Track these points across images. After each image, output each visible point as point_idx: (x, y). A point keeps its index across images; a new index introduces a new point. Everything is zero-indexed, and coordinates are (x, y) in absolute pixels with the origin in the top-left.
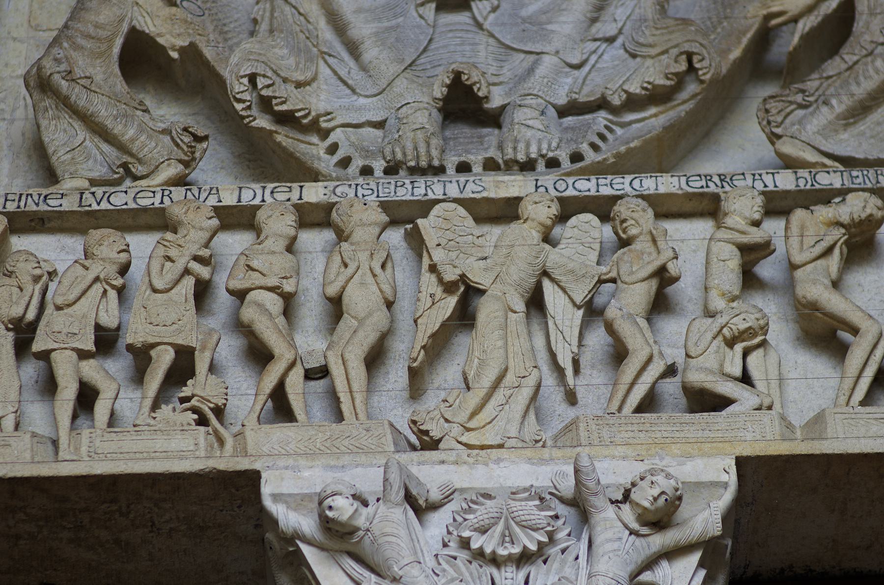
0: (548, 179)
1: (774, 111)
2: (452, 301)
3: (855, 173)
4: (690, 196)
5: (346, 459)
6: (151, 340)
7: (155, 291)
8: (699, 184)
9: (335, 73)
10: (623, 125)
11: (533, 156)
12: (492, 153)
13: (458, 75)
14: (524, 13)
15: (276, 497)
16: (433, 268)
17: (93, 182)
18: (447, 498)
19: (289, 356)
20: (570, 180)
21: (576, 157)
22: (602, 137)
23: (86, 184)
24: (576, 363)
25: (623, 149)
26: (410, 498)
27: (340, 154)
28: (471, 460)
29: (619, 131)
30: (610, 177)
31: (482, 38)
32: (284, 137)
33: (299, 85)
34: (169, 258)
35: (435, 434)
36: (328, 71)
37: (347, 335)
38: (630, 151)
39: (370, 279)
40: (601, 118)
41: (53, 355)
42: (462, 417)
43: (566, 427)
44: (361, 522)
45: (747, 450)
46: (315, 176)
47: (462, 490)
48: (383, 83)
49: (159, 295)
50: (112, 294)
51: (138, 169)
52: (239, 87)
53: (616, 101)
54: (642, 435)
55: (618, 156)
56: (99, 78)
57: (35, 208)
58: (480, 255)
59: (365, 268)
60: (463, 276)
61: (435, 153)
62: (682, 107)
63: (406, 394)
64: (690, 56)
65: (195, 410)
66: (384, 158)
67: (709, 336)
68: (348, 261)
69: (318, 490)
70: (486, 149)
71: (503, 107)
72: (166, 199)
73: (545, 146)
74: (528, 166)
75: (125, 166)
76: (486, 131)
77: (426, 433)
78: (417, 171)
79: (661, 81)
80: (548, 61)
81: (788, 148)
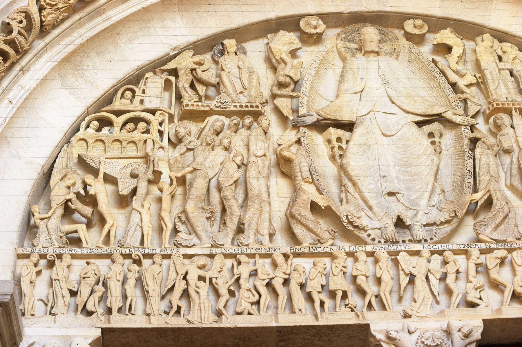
0: (426, 245)
1: (477, 227)
2: (408, 278)
3: (499, 244)
4: (460, 250)
5: (390, 321)
6: (336, 289)
7: (334, 275)
8: (463, 247)
9: (366, 214)
10: (439, 229)
11: (421, 239)
12: (410, 237)
13: (399, 216)
14: (411, 198)
15: (374, 330)
16: (403, 270)
17: (310, 244)
18: (416, 331)
19: (371, 294)
20: (431, 245)
21: (431, 239)
22: (436, 233)
23: (309, 245)
24: (438, 294)
25: (442, 237)
26: (409, 332)
27: (371, 237)
28: (420, 321)
29: (439, 231)
30: (441, 245)
31: (400, 204)
32: (356, 232)
33: (358, 218)
34: (336, 267)
35: (410, 314)
36: (364, 214)
37: (384, 288)
38: (444, 237)
39: (387, 273)
40: (434, 227)
41: (312, 293)
42: (416, 309)
43: (441, 312)
44: (397, 337)
45: (485, 318)
46: (366, 244)
47: (419, 329)
48: (380, 218)
49: (335, 277)
50: (323, 276)
51: (322, 241)
52: (344, 219)
53: (438, 224)
54: (460, 314)
55: (441, 239)
56: (307, 215)
57: (298, 252)
58: (413, 266)
59: (386, 269)
60: (410, 272)
61: (397, 237)
62: (453, 225)
63: (397, 302)
64: (455, 211)
65: (350, 308)
66: (384, 238)
67: (472, 288)
68: (381, 268)
69: (386, 329)
70: (408, 236)
71: (410, 225)
72: (331, 250)
73: (424, 236)
74: (420, 241)
75: (318, 240)
76: (406, 230)
77: (408, 313)
78: (393, 242)
79: (449, 218)
80: (420, 212)
81: (482, 237)
